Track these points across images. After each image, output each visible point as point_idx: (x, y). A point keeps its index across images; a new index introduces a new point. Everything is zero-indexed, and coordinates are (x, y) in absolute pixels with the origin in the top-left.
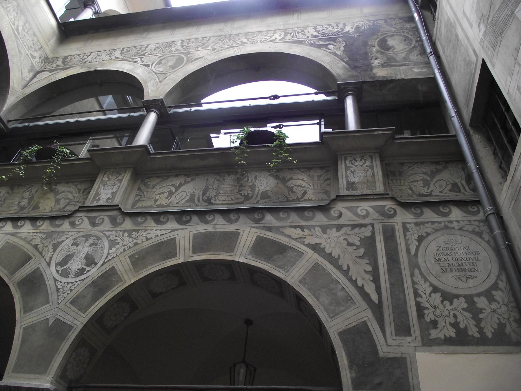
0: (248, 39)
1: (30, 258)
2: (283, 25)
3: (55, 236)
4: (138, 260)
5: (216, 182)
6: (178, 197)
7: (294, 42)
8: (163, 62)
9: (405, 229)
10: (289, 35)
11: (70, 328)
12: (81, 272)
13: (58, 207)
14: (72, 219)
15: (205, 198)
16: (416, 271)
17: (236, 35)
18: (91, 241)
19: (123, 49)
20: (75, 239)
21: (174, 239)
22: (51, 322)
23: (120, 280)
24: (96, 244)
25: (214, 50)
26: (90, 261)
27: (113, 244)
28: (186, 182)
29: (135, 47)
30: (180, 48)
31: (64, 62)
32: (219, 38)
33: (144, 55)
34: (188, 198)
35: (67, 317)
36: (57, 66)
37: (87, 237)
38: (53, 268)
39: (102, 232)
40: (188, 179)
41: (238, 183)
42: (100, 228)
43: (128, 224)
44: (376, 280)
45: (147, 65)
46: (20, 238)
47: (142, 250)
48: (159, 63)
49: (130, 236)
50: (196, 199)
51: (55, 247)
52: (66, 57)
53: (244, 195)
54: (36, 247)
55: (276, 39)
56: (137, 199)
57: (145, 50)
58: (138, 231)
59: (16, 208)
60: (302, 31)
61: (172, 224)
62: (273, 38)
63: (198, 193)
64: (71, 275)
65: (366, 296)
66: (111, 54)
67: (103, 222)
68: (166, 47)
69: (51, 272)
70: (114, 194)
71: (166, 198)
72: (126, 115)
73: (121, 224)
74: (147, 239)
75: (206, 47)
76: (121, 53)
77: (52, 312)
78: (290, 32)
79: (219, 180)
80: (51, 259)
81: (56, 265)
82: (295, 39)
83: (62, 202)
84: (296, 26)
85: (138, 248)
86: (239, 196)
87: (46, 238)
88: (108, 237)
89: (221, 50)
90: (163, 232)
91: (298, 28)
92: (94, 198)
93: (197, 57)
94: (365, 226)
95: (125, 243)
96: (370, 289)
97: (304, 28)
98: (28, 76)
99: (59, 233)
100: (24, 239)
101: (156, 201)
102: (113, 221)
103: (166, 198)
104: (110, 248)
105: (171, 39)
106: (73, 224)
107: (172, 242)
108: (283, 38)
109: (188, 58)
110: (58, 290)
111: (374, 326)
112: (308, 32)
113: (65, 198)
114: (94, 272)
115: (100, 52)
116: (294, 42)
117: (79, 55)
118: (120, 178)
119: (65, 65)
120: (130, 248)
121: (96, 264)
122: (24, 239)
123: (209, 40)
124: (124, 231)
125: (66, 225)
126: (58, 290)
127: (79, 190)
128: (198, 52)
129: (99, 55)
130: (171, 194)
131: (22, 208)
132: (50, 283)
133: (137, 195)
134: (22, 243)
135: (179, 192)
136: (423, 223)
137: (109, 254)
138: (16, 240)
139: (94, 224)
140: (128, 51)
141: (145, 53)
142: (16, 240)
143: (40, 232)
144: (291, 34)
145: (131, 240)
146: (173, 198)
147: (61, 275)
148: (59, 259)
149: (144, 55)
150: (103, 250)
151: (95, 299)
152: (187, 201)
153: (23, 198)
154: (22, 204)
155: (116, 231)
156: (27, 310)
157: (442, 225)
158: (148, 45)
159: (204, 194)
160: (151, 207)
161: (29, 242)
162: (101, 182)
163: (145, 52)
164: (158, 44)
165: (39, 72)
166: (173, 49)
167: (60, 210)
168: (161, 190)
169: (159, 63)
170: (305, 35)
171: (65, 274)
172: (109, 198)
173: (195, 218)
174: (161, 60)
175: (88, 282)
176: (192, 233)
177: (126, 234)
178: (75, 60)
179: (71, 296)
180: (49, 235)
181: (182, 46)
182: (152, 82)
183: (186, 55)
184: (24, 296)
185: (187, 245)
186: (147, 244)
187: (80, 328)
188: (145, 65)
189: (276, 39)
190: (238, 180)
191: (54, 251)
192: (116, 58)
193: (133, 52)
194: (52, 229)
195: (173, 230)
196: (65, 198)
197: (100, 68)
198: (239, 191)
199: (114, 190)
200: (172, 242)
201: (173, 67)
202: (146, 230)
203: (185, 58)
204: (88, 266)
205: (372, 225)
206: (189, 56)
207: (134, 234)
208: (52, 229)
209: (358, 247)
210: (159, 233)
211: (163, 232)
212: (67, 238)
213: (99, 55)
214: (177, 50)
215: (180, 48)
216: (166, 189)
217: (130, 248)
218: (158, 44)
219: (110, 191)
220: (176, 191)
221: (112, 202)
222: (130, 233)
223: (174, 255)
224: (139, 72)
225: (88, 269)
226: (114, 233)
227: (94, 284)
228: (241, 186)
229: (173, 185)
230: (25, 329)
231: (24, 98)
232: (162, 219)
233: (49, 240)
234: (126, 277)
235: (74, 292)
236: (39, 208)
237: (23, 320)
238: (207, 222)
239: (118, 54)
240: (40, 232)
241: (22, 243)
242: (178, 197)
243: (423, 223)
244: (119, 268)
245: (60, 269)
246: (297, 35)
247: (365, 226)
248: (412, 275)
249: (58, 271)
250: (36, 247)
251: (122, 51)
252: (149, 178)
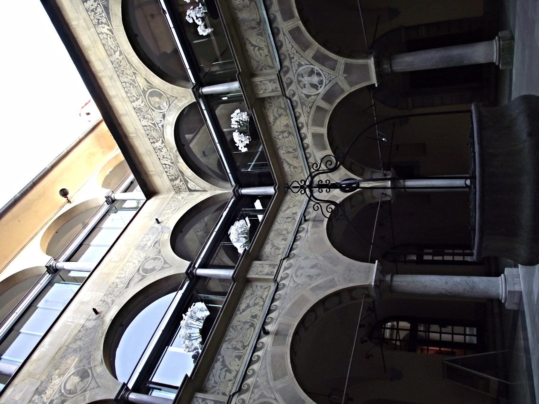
0: (115, 52)
1: (318, 106)
2: (89, 29)
3: (303, 101)
4: (305, 46)
5: (245, 24)
6: (260, 43)
7: (108, 13)
8: (157, 106)
10: (100, 21)
12: (319, 74)
13: (284, 113)
14: (291, 97)
15: (257, 26)
17: (113, 64)
18: (300, 78)
19: (152, 143)
20: (302, 88)
21: (289, 32)
22: (346, 75)
23: (318, 51)
24: (302, 74)
25: (134, 73)
26: (311, 73)
27: (300, 65)
28: (250, 43)
29: (148, 135)
30: (140, 100)
31: (176, 179)
32: (121, 75)
33: (154, 124)
34: (260, 37)
35: (341, 69)
36: (181, 181)
37: (299, 82)
38: (320, 91)
39: (294, 75)
40: (248, 42)
41: (243, 10)
42: (292, 77)
43: (286, 63)
45: (164, 116)
46: (308, 120)
47: (300, 47)
48: (159, 108)
49: (293, 58)
50: (260, 31)
51: (308, 96)
52: (172, 180)
53: (250, 3)
54: (311, 108)
55: (108, 29)
56: (268, 68)
57: (149, 126)
58: (289, 55)
59: (290, 137)
60: (93, 11)
61: (281, 37)
62: (108, 32)
63: (255, 32)
64: (321, 79)
66: (159, 149)
67: (288, 78)
68: (142, 111)
69: (322, 90)
70: (270, 81)
71: (263, 50)
72: (205, 112)
73: (287, 67)
74: (293, 47)
75: (134, 81)
76: (157, 141)
77: (340, 77)
78: (97, 21)
79: (244, 23)
80: (315, 95)
81: (318, 90)
82: (104, 14)
83: (280, 113)
84: (88, 18)
85: (299, 50)
86: (252, 6)
87: (305, 105)
88: (296, 70)
89: (133, 67)
90: (287, 40)
91: (90, 16)
92: (275, 91)
93: (145, 83)
95: (298, 58)
97: (87, 11)
98: (196, 194)
99: (300, 99)
100: (308, 117)
101: (266, 56)
102: (287, 72)
103: (263, 50)
104: (303, 65)
105: (133, 112)
106: (294, 95)
107: (292, 32)
108: (105, 24)
109: (148, 89)
110: (330, 81)
112: (92, 5)
113: (278, 112)
114: (317, 67)
115: (159, 159)
116: (108, 13)
117: (166, 172)
118: (259, 83)
119: (179, 176)
120: (300, 54)
121: (312, 68)
122: (308, 117)
123: (125, 82)
124: (291, 62)
125: (295, 98)
126: (330, 81)
127: (271, 106)
128: (141, 84)
129: (163, 157)
130: (260, 49)
131: (290, 133)
132: (328, 88)
133: (266, 69)
134: (311, 117)
135: (257, 44)
137: (306, 64)
138: (310, 121)
139: (291, 82)
140: (154, 138)
141: (152, 124)
142: (310, 121)
143: (302, 110)
144: (99, 20)
145: (295, 56)
146: (262, 46)
147: (322, 84)
148: (314, 90)
149: (154, 124)
150: (304, 69)
151: (330, 59)
152: (262, 36)
153: (283, 137)
154: (287, 135)
155: (292, 67)
156: (343, 91)
158: (143, 126)
159: (255, 28)
160: (271, 57)
161: (309, 113)
162: (264, 93)
163: (151, 125)
164: (140, 119)
165: (190, 190)
166: (142, 105)
167: (285, 111)
168: (259, 56)
169: (159, 108)
170: (96, 7)
171: (321, 82)
172: (274, 82)
173: (274, 25)
174: (156, 108)
175: (323, 68)
176: (284, 23)
177: (293, 61)
178: (172, 171)
179: (331, 72)
180: (303, 104)
181: (137, 99)
182: (178, 104)
183: (147, 92)
184: (337, 97)
185: (291, 23)
186: (296, 46)
187: (345, 59)
188: (164, 118)
189: (108, 29)
190: (241, 10)
191: (311, 96)
192: (163, 142)
193: (154, 134)
194: (299, 105)
195: (284, 35)
196: (278, 112)
197: (176, 148)
198: (248, 7)
199: (268, 82)
200: (292, 32)
201: (160, 95)
202: (288, 50)
203: (149, 91)
204: (314, 72)
206: (146, 89)
207: (292, 56)
208: (299, 105)
210: (287, 42)
211: (287, 40)
213: (163, 157)
214: (142, 102)
215: (140, 100)
216: (258, 53)
217: (300, 54)
218: (140, 119)
219: (269, 84)
220: (257, 46)
221: (276, 79)
222: (291, 59)
223: (298, 28)
224: (172, 118)
225: (316, 72)
226: (293, 68)
227: (323, 64)
228: (244, 7)
229: (254, 50)
230: (351, 86)
231: (214, 185)
232: (279, 44)
233: (306, 103)
234: (316, 48)
235: (329, 72)
236: (287, 124)
237: (348, 90)
238: (275, 17)
239: (158, 144)
240: (302, 110)
241: (311, 117)
242: (260, 43)
244: (311, 55)
245: (319, 86)
246: (98, 14)
249: (321, 87)
250: (311, 108)
251: (154, 142)
252: (252, 67)
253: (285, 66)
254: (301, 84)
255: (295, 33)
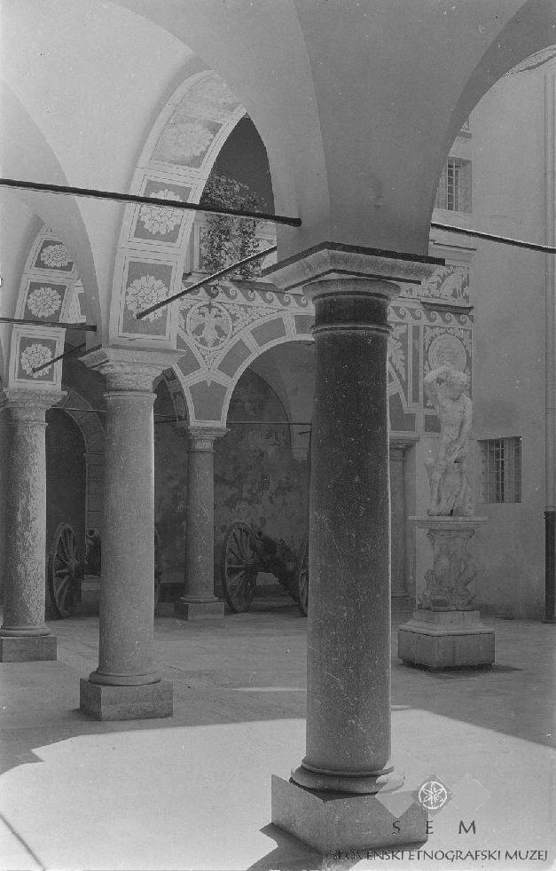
4: (261, 334)
9: (425, 331)
11: (226, 388)
12: (216, 343)
16: (427, 363)
20: (199, 308)
44: (406, 367)
65: (399, 376)
69: (191, 341)
94: (403, 324)
96: (402, 371)
111: (402, 396)
114: (228, 344)
124: (241, 306)
136: (435, 327)
148: (194, 327)
157: (444, 331)
179: (219, 361)
195: (279, 310)
205: (407, 324)
209: (398, 341)
212: (192, 306)
225: (222, 339)
243: (435, 327)
247: (403, 324)
248: (424, 364)
253: (236, 295)
254: (206, 310)
255: (277, 327)
